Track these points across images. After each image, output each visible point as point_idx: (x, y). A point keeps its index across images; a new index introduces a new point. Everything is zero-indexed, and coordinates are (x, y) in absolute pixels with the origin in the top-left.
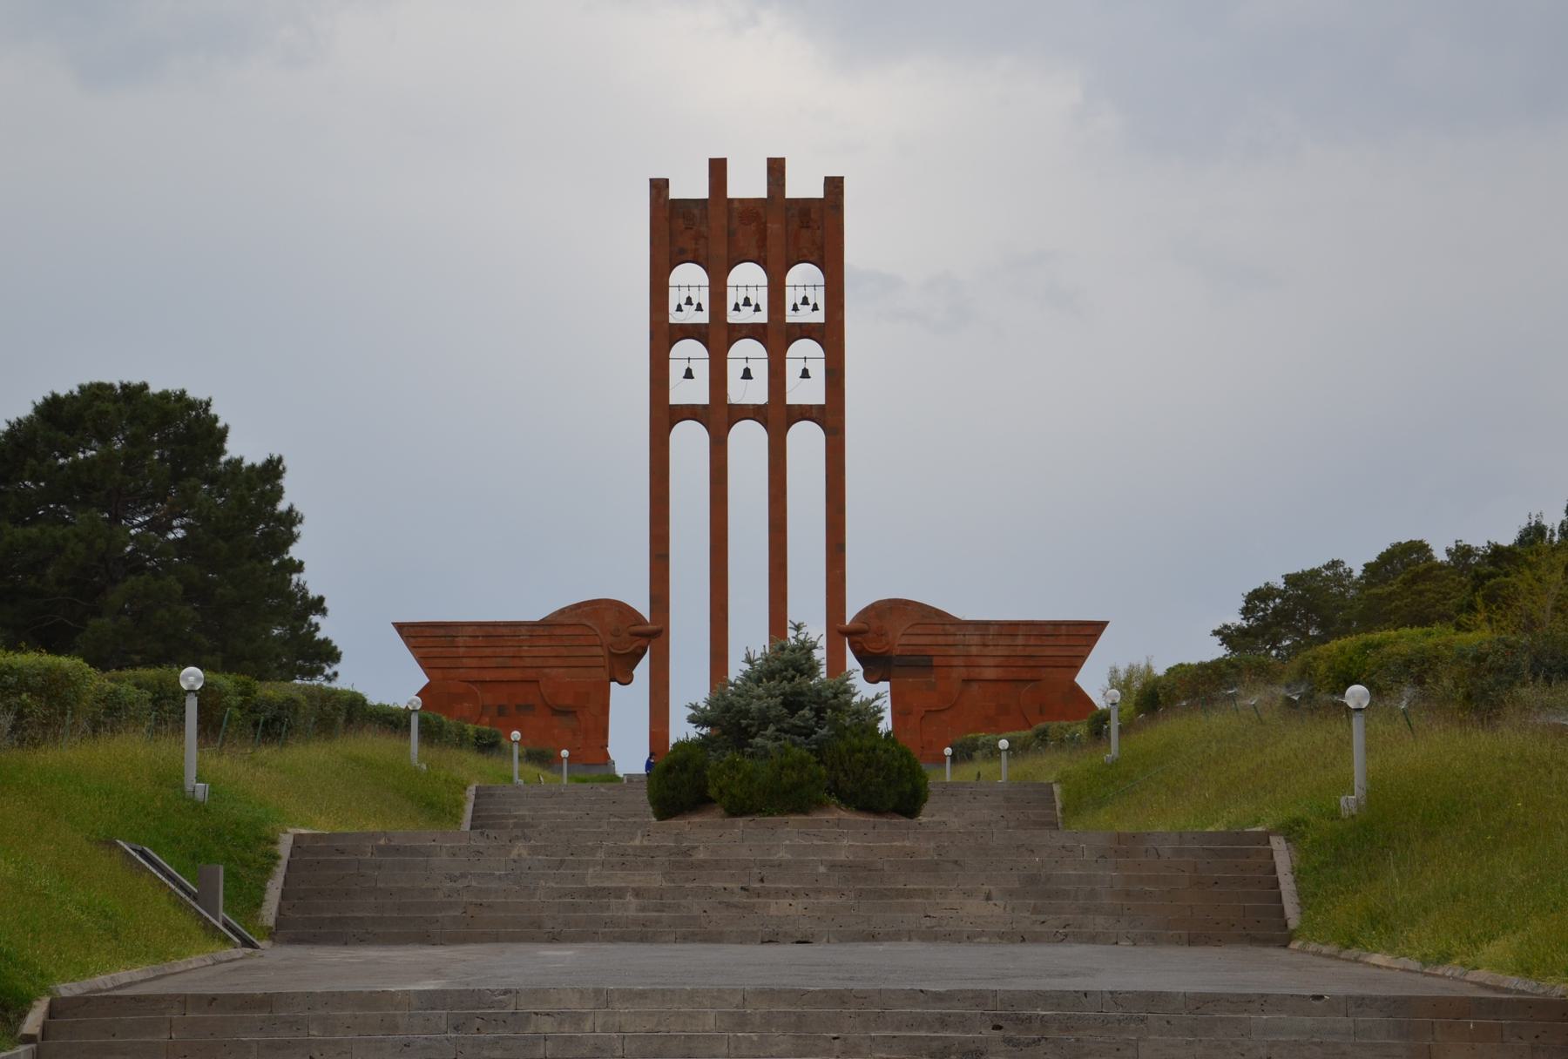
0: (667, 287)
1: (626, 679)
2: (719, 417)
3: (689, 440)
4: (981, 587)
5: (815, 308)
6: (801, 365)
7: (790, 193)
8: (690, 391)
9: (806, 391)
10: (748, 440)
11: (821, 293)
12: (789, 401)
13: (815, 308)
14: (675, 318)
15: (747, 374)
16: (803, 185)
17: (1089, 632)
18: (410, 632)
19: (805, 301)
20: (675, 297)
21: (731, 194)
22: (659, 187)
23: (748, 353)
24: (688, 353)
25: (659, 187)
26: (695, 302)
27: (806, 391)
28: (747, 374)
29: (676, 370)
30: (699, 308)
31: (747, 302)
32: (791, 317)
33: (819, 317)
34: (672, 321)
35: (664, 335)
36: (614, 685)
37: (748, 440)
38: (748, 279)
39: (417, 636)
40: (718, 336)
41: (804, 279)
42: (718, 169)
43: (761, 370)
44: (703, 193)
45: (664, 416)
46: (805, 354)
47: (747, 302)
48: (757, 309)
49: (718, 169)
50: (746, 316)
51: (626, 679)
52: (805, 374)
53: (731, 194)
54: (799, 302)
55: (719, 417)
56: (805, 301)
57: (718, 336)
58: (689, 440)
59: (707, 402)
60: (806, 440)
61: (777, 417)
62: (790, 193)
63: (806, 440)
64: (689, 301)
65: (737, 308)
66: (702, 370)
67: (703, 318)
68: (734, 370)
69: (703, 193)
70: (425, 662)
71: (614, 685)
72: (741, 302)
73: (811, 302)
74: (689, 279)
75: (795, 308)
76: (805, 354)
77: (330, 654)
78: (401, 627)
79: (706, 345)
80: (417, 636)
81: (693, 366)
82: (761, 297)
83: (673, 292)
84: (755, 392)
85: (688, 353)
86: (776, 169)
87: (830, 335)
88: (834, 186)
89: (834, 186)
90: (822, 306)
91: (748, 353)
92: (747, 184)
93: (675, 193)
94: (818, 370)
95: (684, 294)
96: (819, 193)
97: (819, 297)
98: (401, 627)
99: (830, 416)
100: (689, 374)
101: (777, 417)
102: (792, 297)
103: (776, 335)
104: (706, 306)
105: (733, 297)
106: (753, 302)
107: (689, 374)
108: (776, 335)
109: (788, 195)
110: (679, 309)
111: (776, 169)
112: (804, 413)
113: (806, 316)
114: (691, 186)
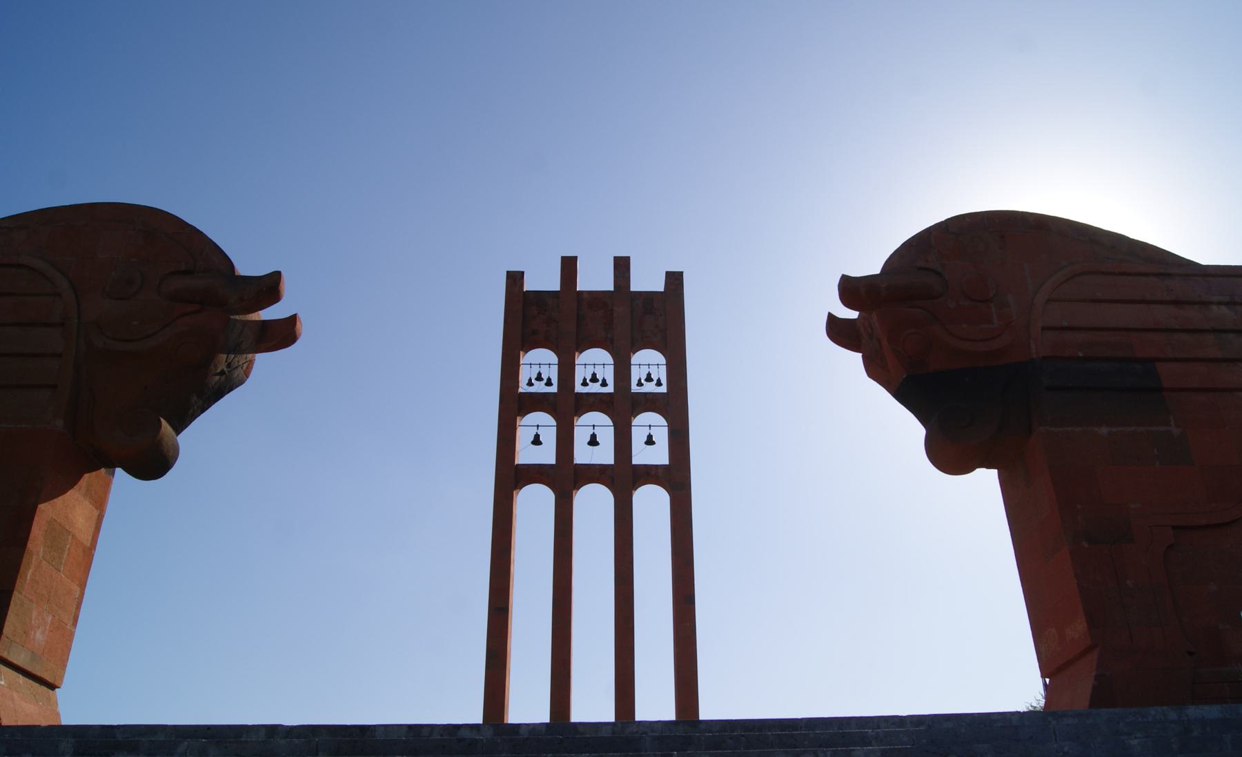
0: (518, 365)
2: (565, 478)
3: (534, 504)
5: (659, 384)
6: (646, 432)
7: (634, 287)
10: (593, 504)
11: (663, 369)
12: (635, 462)
14: (523, 388)
15: (593, 442)
16: (646, 280)
19: (649, 379)
20: (525, 374)
21: (580, 287)
22: (515, 279)
23: (594, 423)
25: (515, 279)
28: (593, 442)
30: (549, 383)
32: (635, 388)
33: (663, 389)
34: (521, 390)
35: (514, 404)
37: (593, 504)
38: (594, 365)
40: (566, 405)
41: (648, 365)
42: (569, 266)
43: (607, 436)
46: (649, 424)
47: (594, 379)
48: (604, 384)
49: (569, 266)
53: (580, 287)
55: (565, 478)
56: (649, 379)
57: (566, 405)
58: (534, 504)
59: (553, 462)
60: (651, 504)
61: (623, 478)
62: (634, 287)
63: (651, 504)
64: (539, 378)
65: (585, 384)
66: (550, 436)
69: (556, 287)
72: (589, 378)
74: (539, 365)
75: (640, 384)
76: (649, 424)
81: (541, 431)
82: (608, 374)
84: (604, 455)
85: (540, 423)
86: (622, 266)
87: (673, 405)
88: (675, 280)
89: (675, 280)
90: (664, 381)
91: (594, 423)
92: (595, 278)
93: (529, 285)
95: (535, 370)
96: (659, 286)
97: (661, 373)
99: (675, 477)
101: (623, 478)
102: (637, 374)
103: (622, 405)
104: (555, 381)
105: (580, 374)
106: (600, 377)
108: (622, 405)
109: (633, 289)
111: (622, 266)
112: (649, 474)
113: (650, 388)
114: (543, 279)
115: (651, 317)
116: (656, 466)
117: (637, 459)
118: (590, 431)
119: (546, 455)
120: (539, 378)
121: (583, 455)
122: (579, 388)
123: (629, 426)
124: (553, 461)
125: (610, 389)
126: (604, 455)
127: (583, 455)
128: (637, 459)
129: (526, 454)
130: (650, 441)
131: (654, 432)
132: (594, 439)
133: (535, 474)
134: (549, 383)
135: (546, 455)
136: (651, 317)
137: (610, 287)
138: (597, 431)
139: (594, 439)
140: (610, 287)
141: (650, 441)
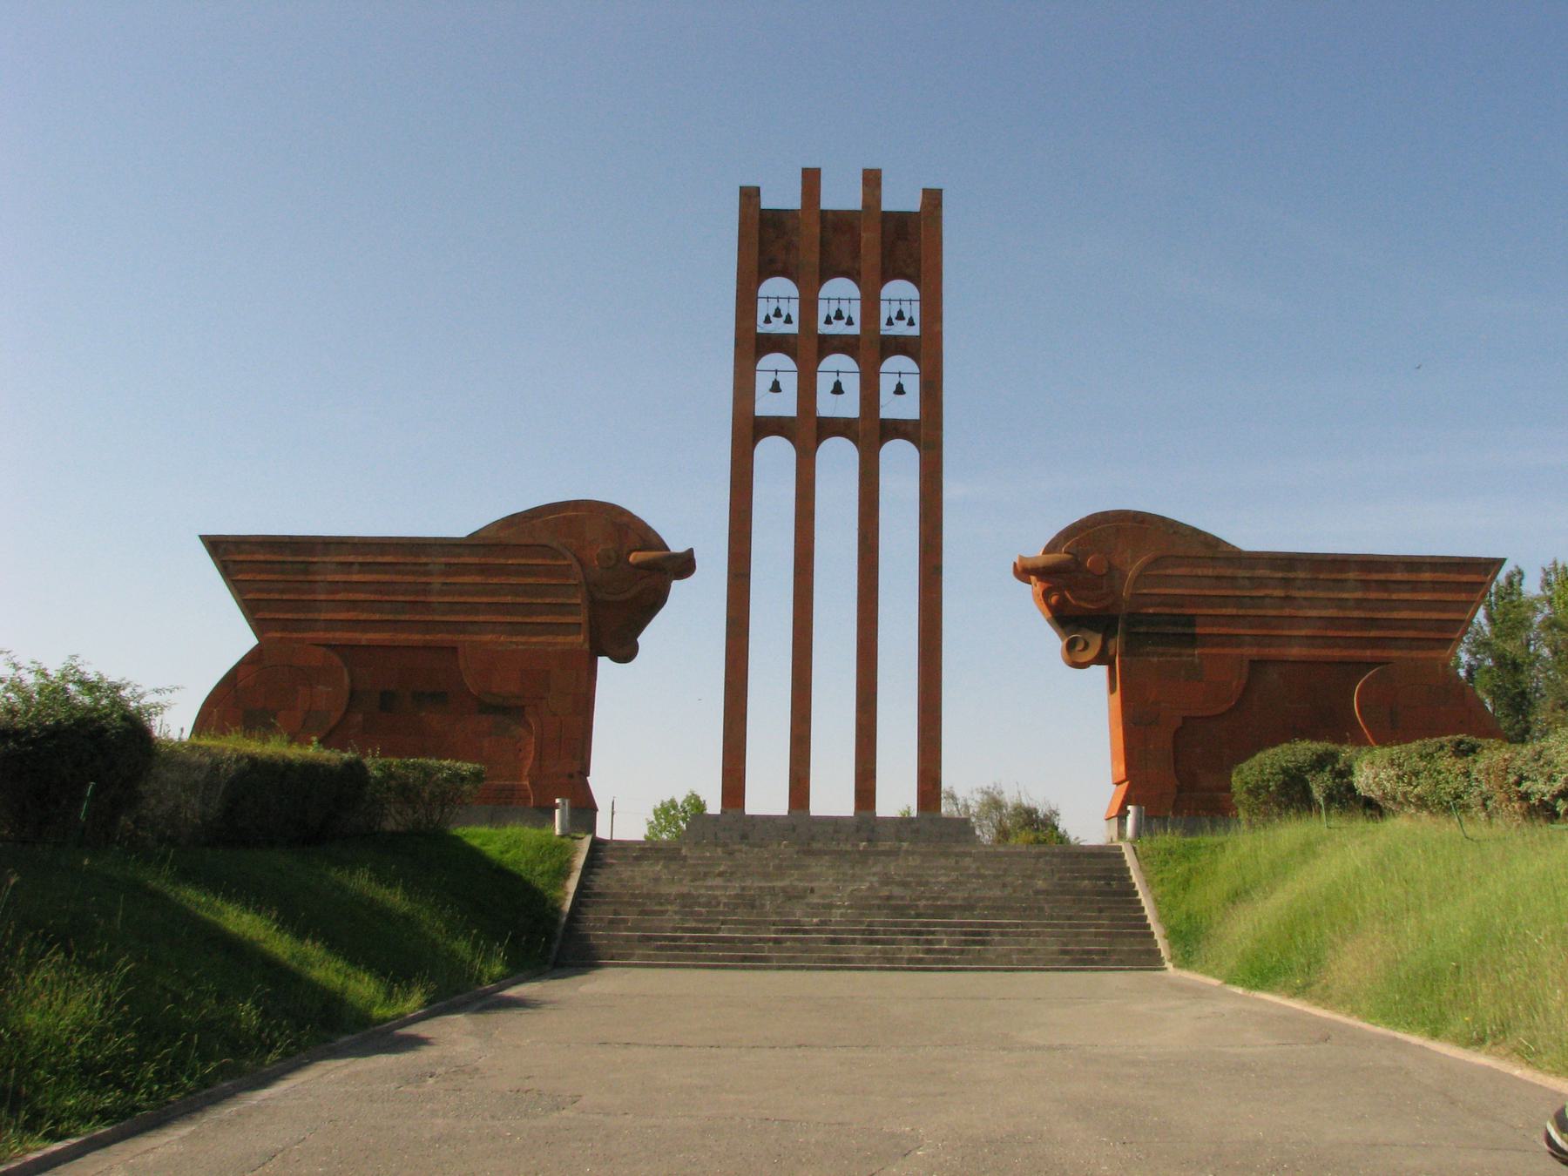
1: (625, 652)
2: (808, 431)
3: (775, 456)
5: (911, 323)
6: (895, 380)
7: (886, 206)
8: (777, 404)
9: (901, 407)
10: (837, 461)
11: (916, 305)
13: (911, 323)
14: (762, 328)
15: (837, 389)
16: (900, 198)
18: (239, 559)
19: (900, 316)
20: (764, 309)
22: (749, 196)
24: (776, 364)
25: (749, 196)
26: (784, 314)
28: (837, 389)
29: (763, 382)
30: (788, 320)
31: (839, 316)
32: (885, 330)
33: (915, 331)
34: (759, 330)
35: (753, 345)
36: (604, 663)
37: (837, 461)
38: (840, 293)
40: (809, 348)
41: (900, 294)
42: (811, 179)
43: (852, 384)
44: (796, 204)
45: (750, 429)
47: (839, 316)
48: (850, 322)
49: (811, 179)
51: (625, 652)
52: (900, 390)
54: (894, 315)
55: (808, 431)
56: (900, 316)
57: (809, 348)
58: (775, 456)
60: (899, 460)
61: (870, 433)
63: (899, 460)
64: (778, 313)
65: (828, 321)
66: (790, 383)
67: (793, 329)
68: (824, 383)
69: (796, 204)
70: (252, 610)
71: (604, 663)
72: (833, 315)
73: (907, 315)
74: (779, 292)
75: (890, 322)
78: (222, 549)
79: (794, 356)
82: (854, 310)
83: (761, 304)
84: (847, 407)
86: (872, 180)
87: (926, 350)
88: (933, 199)
89: (933, 199)
90: (917, 320)
92: (842, 195)
93: (766, 203)
94: (913, 385)
96: (913, 204)
97: (914, 311)
98: (222, 549)
99: (926, 434)
100: (776, 388)
101: (870, 433)
102: (886, 311)
103: (871, 349)
104: (795, 318)
105: (824, 309)
106: (845, 315)
107: (776, 388)
108: (871, 349)
110: (768, 320)
111: (872, 180)
112: (895, 429)
113: (900, 329)
114: (782, 195)
115: (902, 244)
116: (905, 421)
118: (834, 378)
119: (784, 405)
120: (778, 313)
121: (828, 406)
122: (823, 329)
123: (877, 374)
124: (794, 413)
125: (855, 330)
128: (885, 413)
129: (768, 405)
131: (905, 380)
133: (776, 426)
134: (788, 320)
136: (902, 244)
137: (858, 206)
138: (843, 378)
140: (858, 206)
141: (900, 390)
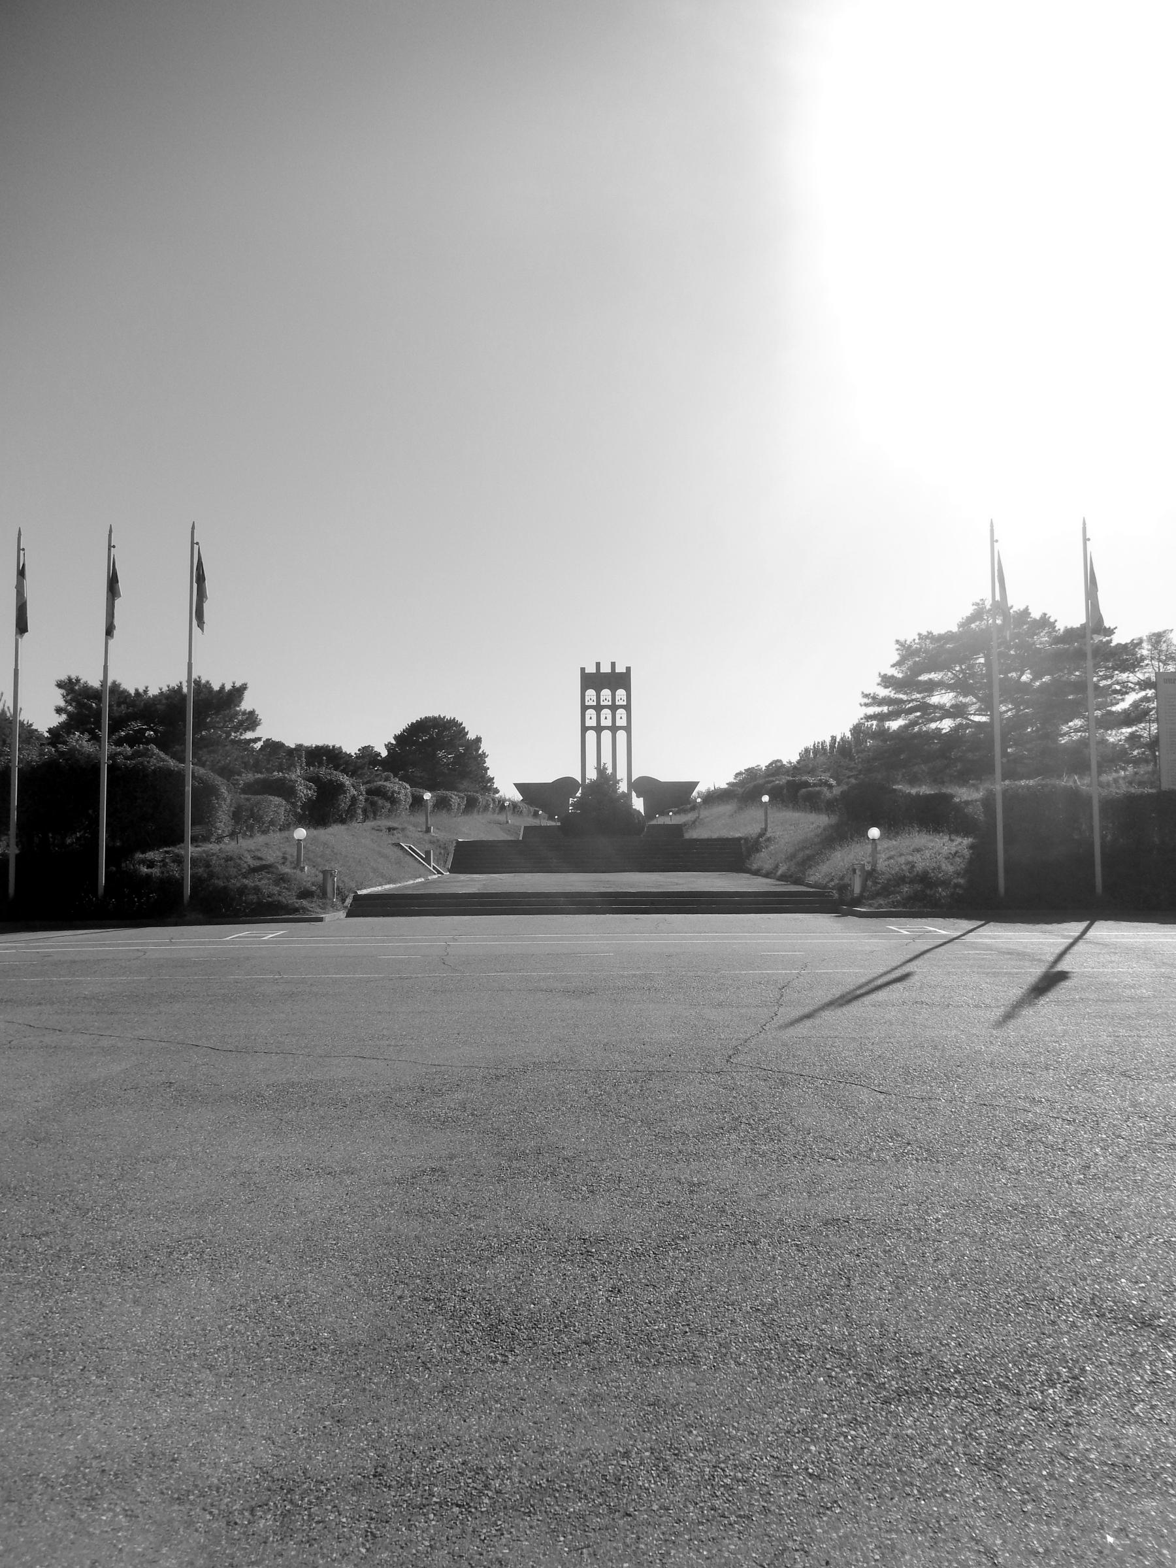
2: (599, 729)
3: (591, 736)
4: (667, 773)
10: (606, 735)
16: (620, 669)
17: (695, 784)
18: (517, 785)
20: (587, 698)
22: (583, 670)
23: (606, 713)
24: (591, 713)
25: (583, 670)
27: (621, 722)
29: (587, 717)
35: (584, 708)
37: (606, 735)
38: (606, 693)
39: (520, 787)
40: (598, 708)
41: (621, 693)
42: (598, 665)
45: (584, 729)
46: (621, 713)
49: (598, 665)
50: (606, 703)
55: (599, 729)
57: (598, 708)
58: (591, 736)
61: (614, 729)
63: (621, 735)
68: (602, 717)
74: (591, 693)
76: (621, 713)
77: (497, 791)
80: (520, 787)
84: (608, 723)
85: (591, 713)
86: (613, 664)
87: (627, 708)
88: (628, 669)
89: (628, 669)
91: (606, 713)
92: (606, 669)
99: (628, 729)
101: (614, 729)
103: (614, 708)
105: (602, 698)
108: (614, 708)
111: (613, 664)
114: (591, 669)
117: (618, 724)
119: (593, 723)
121: (604, 723)
126: (608, 723)
127: (604, 723)
128: (618, 724)
130: (621, 718)
132: (606, 718)
135: (593, 723)
136: (619, 680)
139: (606, 718)
